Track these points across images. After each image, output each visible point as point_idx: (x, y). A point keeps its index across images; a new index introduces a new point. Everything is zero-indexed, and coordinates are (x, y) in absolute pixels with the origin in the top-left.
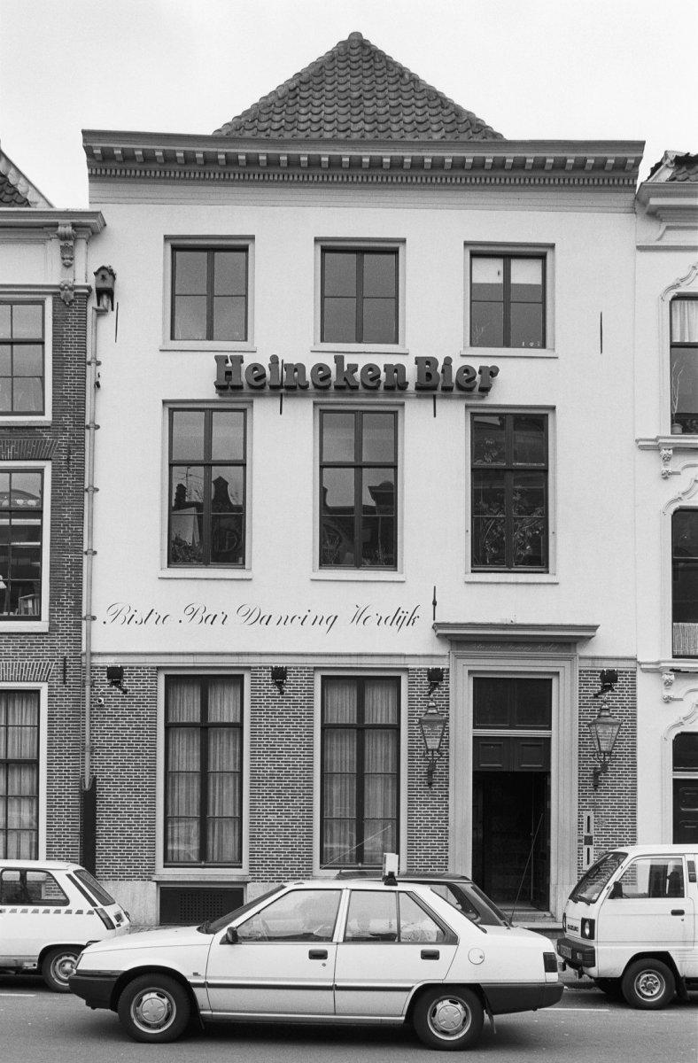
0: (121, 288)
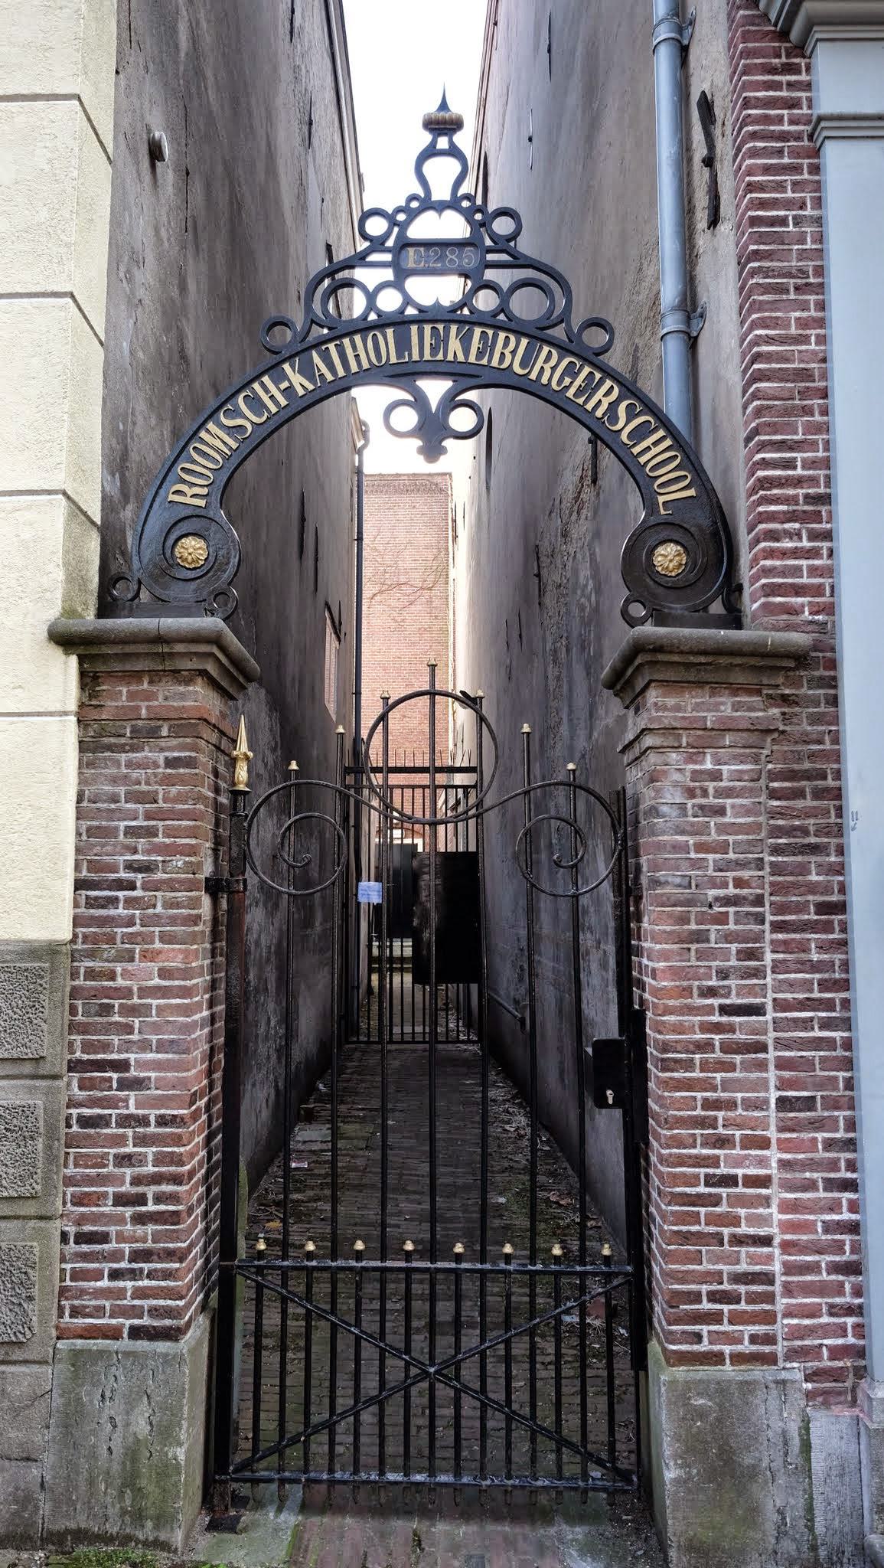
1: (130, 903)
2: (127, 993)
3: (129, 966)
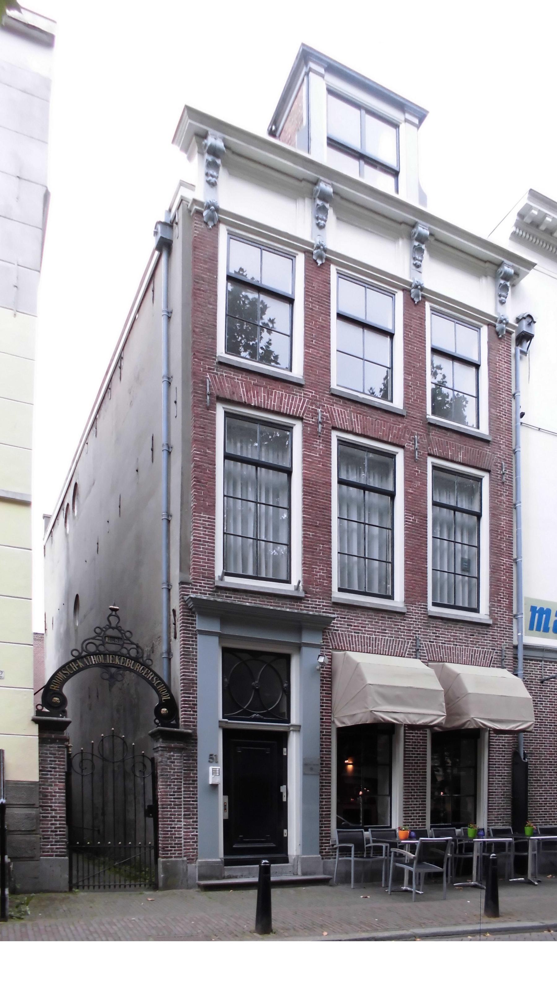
0: (536, 330)
3: (52, 787)
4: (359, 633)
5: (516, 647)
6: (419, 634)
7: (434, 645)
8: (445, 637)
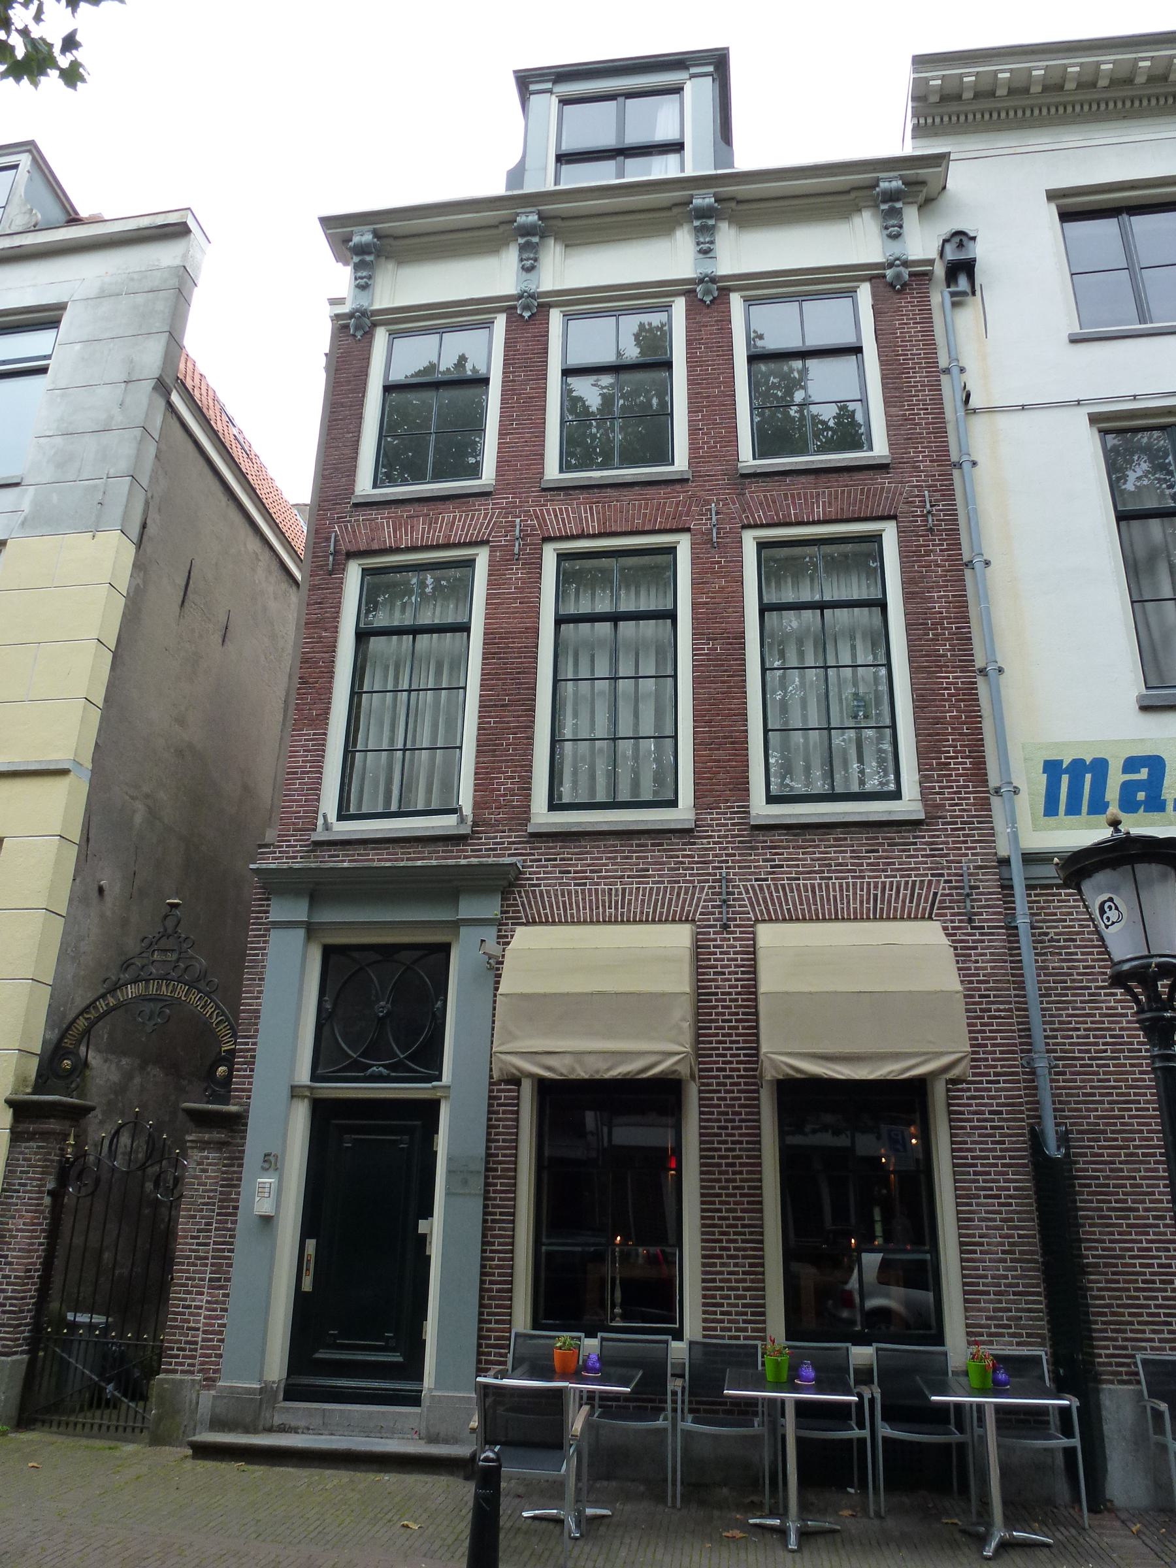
1: (18, 1197)
2: (10, 1230)
4: (585, 884)
5: (1005, 862)
6: (727, 868)
7: (769, 886)
8: (797, 866)
